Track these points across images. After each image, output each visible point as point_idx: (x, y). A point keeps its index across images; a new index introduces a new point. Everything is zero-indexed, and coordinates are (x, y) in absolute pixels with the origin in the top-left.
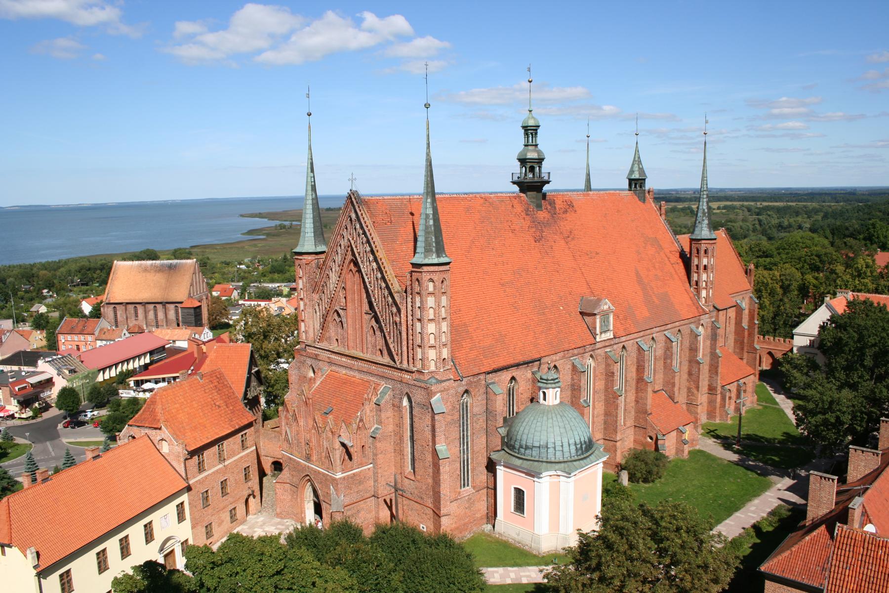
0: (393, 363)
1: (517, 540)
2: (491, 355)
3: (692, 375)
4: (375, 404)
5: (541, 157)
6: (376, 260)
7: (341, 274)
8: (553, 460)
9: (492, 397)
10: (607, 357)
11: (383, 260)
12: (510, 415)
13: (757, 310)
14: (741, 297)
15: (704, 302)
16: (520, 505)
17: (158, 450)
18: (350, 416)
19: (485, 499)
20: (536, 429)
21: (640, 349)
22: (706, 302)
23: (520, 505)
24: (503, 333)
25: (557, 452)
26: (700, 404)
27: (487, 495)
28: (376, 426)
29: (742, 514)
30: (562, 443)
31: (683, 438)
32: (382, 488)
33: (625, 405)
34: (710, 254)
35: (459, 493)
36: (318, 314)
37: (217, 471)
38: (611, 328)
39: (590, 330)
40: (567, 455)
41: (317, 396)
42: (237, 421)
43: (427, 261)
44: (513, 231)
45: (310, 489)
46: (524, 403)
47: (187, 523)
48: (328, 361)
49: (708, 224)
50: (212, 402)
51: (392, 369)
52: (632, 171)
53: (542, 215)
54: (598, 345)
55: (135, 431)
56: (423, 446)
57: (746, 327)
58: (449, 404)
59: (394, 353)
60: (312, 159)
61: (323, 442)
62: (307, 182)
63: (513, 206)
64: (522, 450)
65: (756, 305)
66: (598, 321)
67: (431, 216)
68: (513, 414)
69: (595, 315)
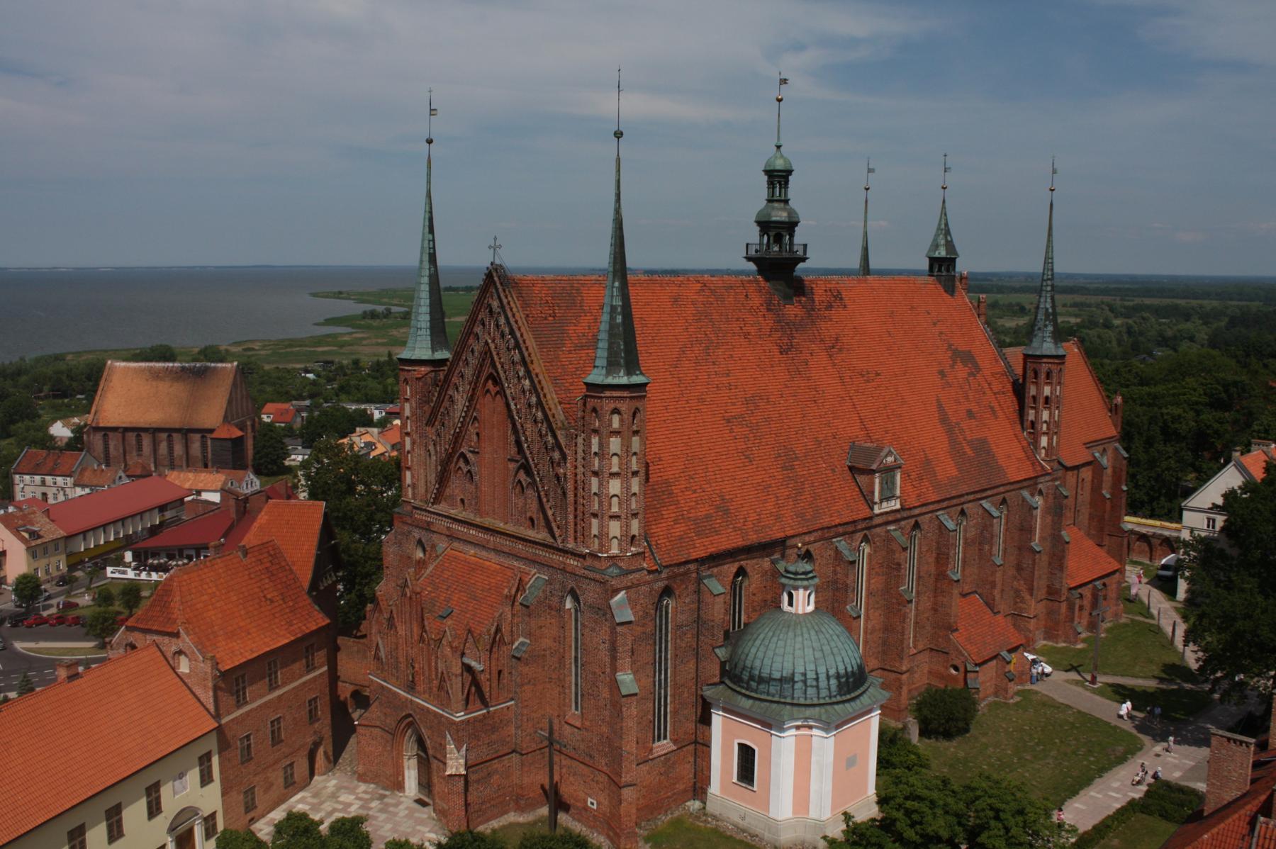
0: (552, 540)
1: (740, 826)
2: (707, 531)
3: (1022, 569)
4: (521, 604)
5: (795, 220)
6: (528, 372)
7: (472, 396)
8: (802, 701)
9: (707, 598)
10: (889, 539)
11: (541, 377)
12: (734, 628)
13: (1124, 468)
14: (1101, 448)
15: (1043, 455)
16: (746, 770)
17: (173, 669)
18: (479, 622)
19: (692, 760)
20: (777, 651)
21: (941, 526)
22: (1047, 455)
23: (746, 770)
24: (727, 497)
25: (809, 689)
26: (1035, 617)
27: (695, 753)
28: (521, 639)
29: (1098, 793)
30: (817, 674)
31: (1007, 670)
32: (528, 737)
33: (916, 616)
34: (1055, 380)
35: (651, 750)
36: (434, 458)
37: (265, 704)
38: (898, 493)
39: (864, 496)
40: (824, 693)
41: (429, 589)
42: (300, 625)
43: (610, 380)
44: (747, 335)
45: (414, 738)
46: (758, 608)
47: (215, 787)
48: (448, 533)
49: (1053, 332)
50: (261, 594)
51: (549, 550)
52: (936, 246)
53: (793, 311)
54: (877, 521)
55: (135, 638)
56: (595, 673)
57: (1108, 496)
58: (638, 607)
59: (554, 525)
60: (431, 212)
61: (436, 663)
62: (423, 247)
63: (746, 296)
64: (754, 684)
65: (1125, 462)
66: (877, 481)
67: (619, 309)
68: (739, 626)
69: (873, 472)
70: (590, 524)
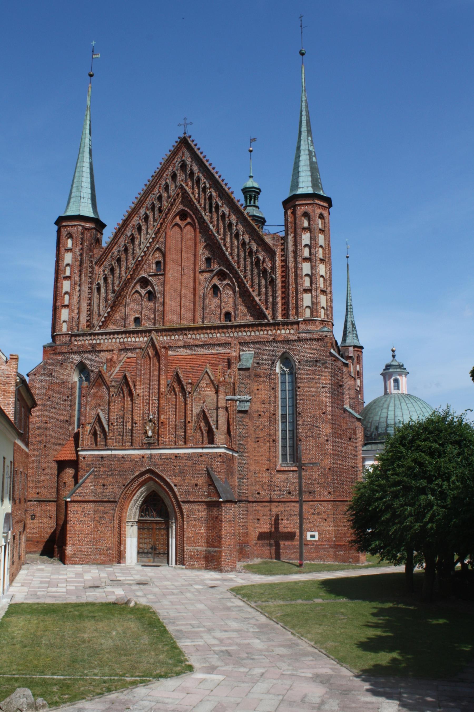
7: (159, 229)
70: (303, 298)
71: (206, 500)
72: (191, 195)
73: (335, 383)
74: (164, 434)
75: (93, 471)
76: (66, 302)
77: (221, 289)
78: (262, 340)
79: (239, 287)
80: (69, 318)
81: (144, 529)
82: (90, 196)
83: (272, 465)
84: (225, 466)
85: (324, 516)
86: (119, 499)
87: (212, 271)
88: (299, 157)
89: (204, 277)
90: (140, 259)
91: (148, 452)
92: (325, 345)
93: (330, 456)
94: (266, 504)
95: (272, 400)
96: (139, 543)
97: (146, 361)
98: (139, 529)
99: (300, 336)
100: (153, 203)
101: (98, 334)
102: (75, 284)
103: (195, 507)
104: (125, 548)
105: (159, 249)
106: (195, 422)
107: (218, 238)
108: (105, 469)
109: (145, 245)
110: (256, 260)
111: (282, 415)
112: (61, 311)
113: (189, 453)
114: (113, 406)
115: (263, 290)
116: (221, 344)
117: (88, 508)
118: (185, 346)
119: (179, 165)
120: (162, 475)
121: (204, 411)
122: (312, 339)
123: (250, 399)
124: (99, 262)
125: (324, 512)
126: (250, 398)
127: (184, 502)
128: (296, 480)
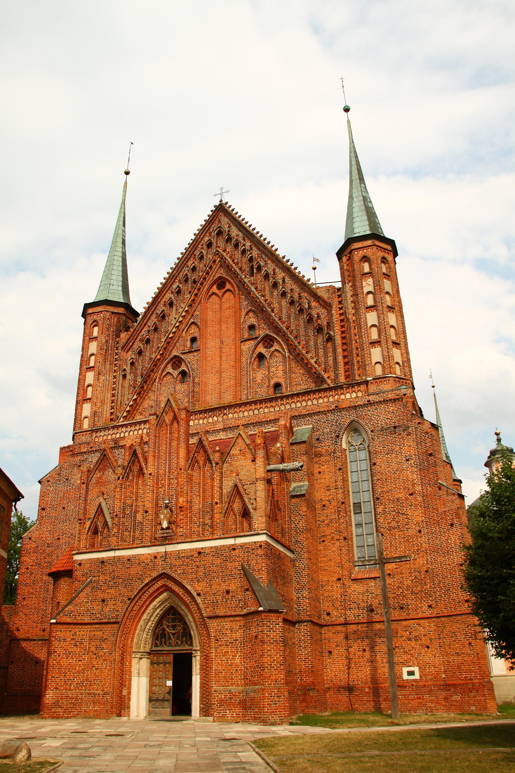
70: (370, 354)
71: (242, 613)
72: (229, 259)
73: (422, 453)
74: (183, 523)
75: (91, 581)
76: (89, 396)
77: (268, 357)
78: (322, 410)
79: (289, 352)
80: (91, 412)
81: (158, 663)
82: (120, 284)
83: (346, 573)
84: (268, 562)
85: (425, 641)
86: (123, 619)
87: (256, 338)
88: (352, 204)
89: (247, 346)
90: (171, 335)
91: (161, 549)
92: (404, 406)
93: (426, 553)
94: (339, 628)
95: (340, 484)
96: (151, 685)
97: (163, 430)
98: (152, 663)
99: (371, 398)
100: (186, 275)
101: (122, 426)
102: (99, 374)
103: (227, 624)
104: (129, 693)
105: (193, 323)
106: (226, 502)
107: (261, 299)
108: (105, 577)
109: (177, 320)
110: (308, 318)
111: (354, 504)
112: (82, 406)
113: (217, 547)
114: (118, 492)
115: (321, 352)
116: (270, 421)
117: (82, 633)
118: (225, 428)
119: (216, 233)
120: (181, 580)
121: (236, 486)
122: (387, 401)
123: (302, 467)
124: (126, 347)
125: (424, 636)
126: (301, 464)
127: (209, 618)
128: (379, 592)
